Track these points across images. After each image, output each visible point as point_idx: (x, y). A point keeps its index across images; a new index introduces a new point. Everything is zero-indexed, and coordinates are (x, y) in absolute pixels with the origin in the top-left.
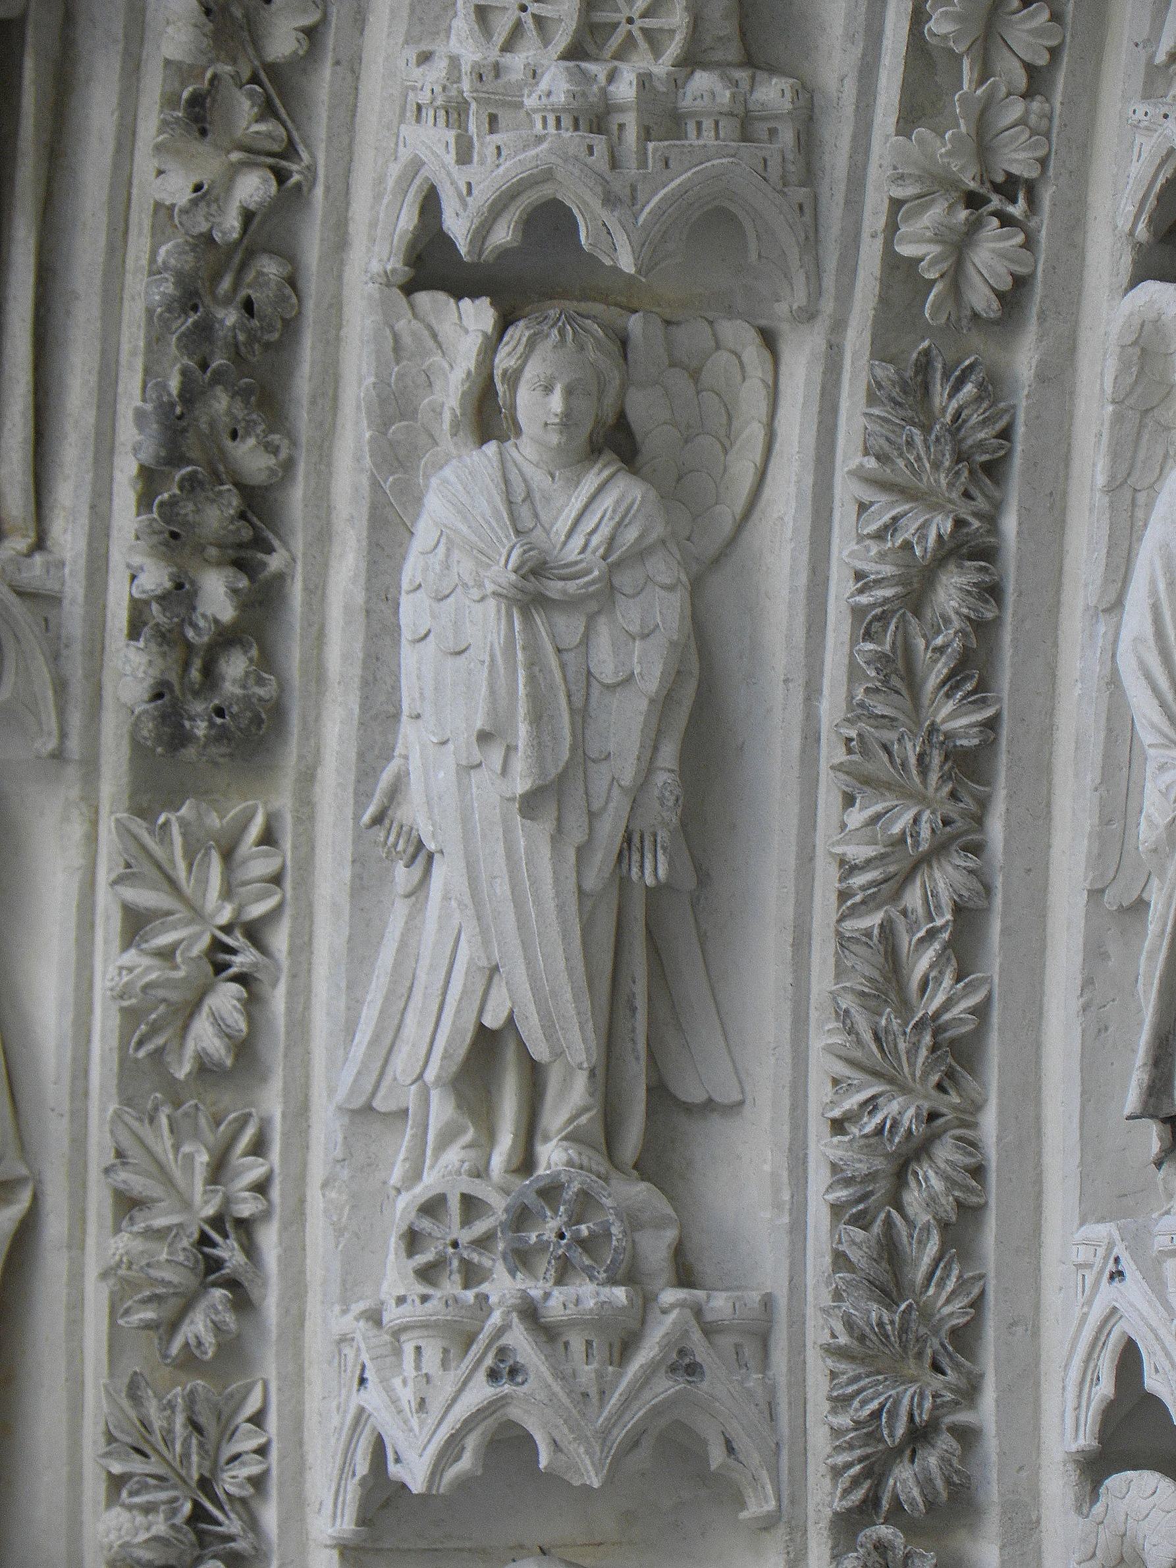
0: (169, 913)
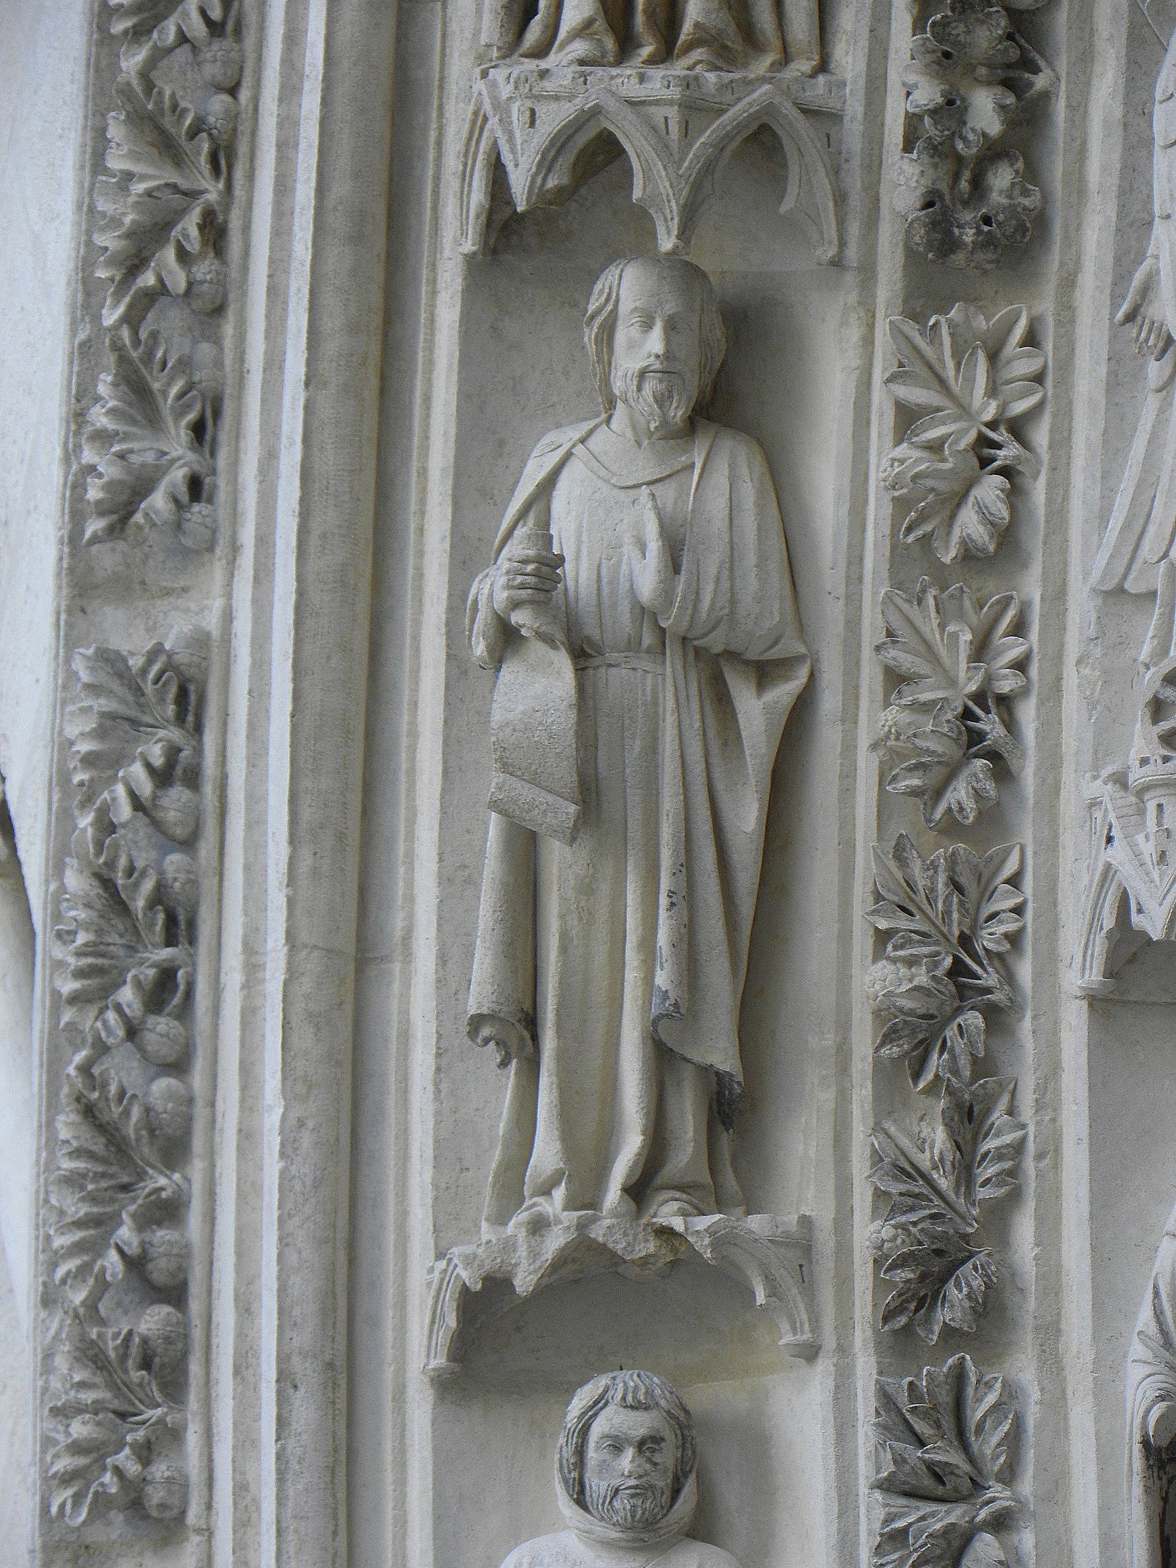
0: (938, 410)
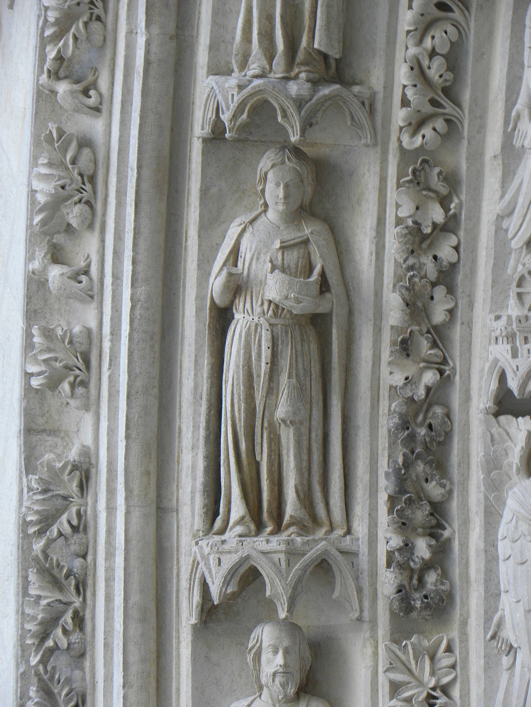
0: (409, 683)
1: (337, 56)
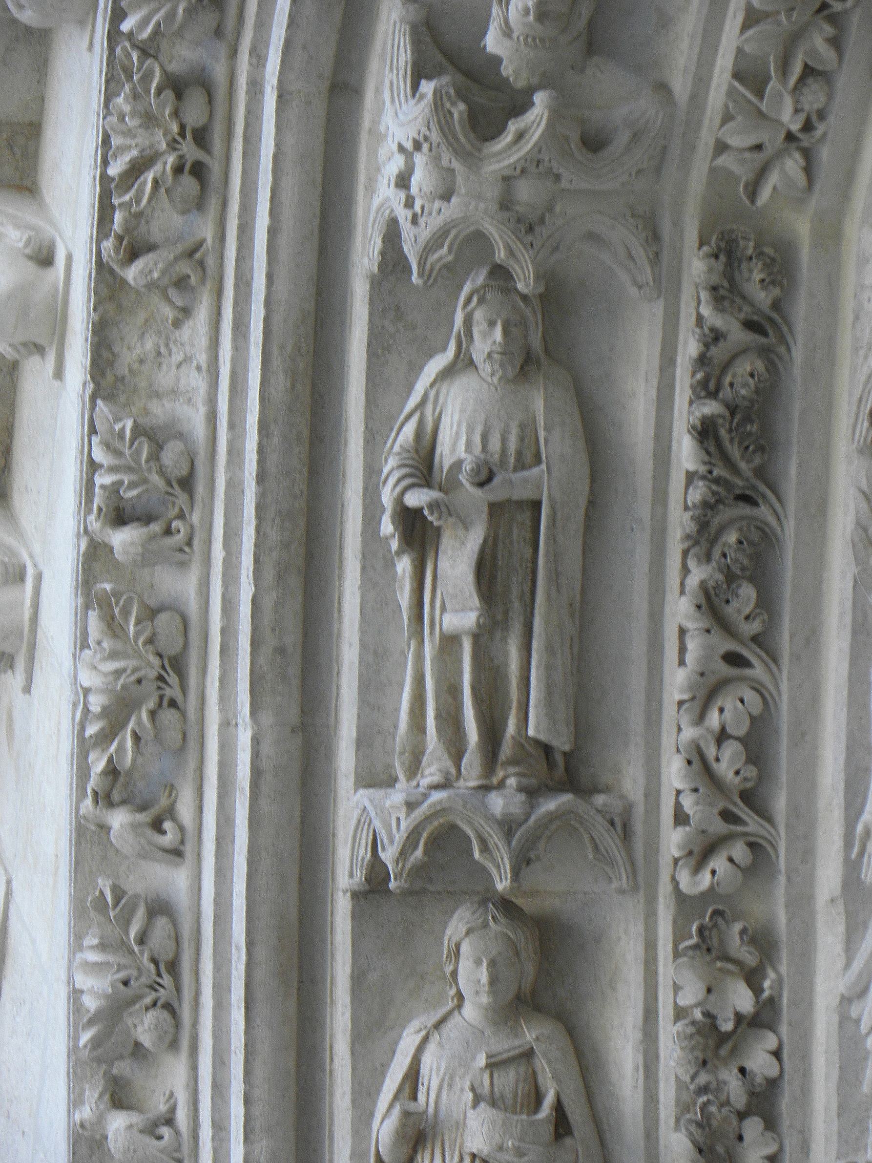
1: (567, 748)
